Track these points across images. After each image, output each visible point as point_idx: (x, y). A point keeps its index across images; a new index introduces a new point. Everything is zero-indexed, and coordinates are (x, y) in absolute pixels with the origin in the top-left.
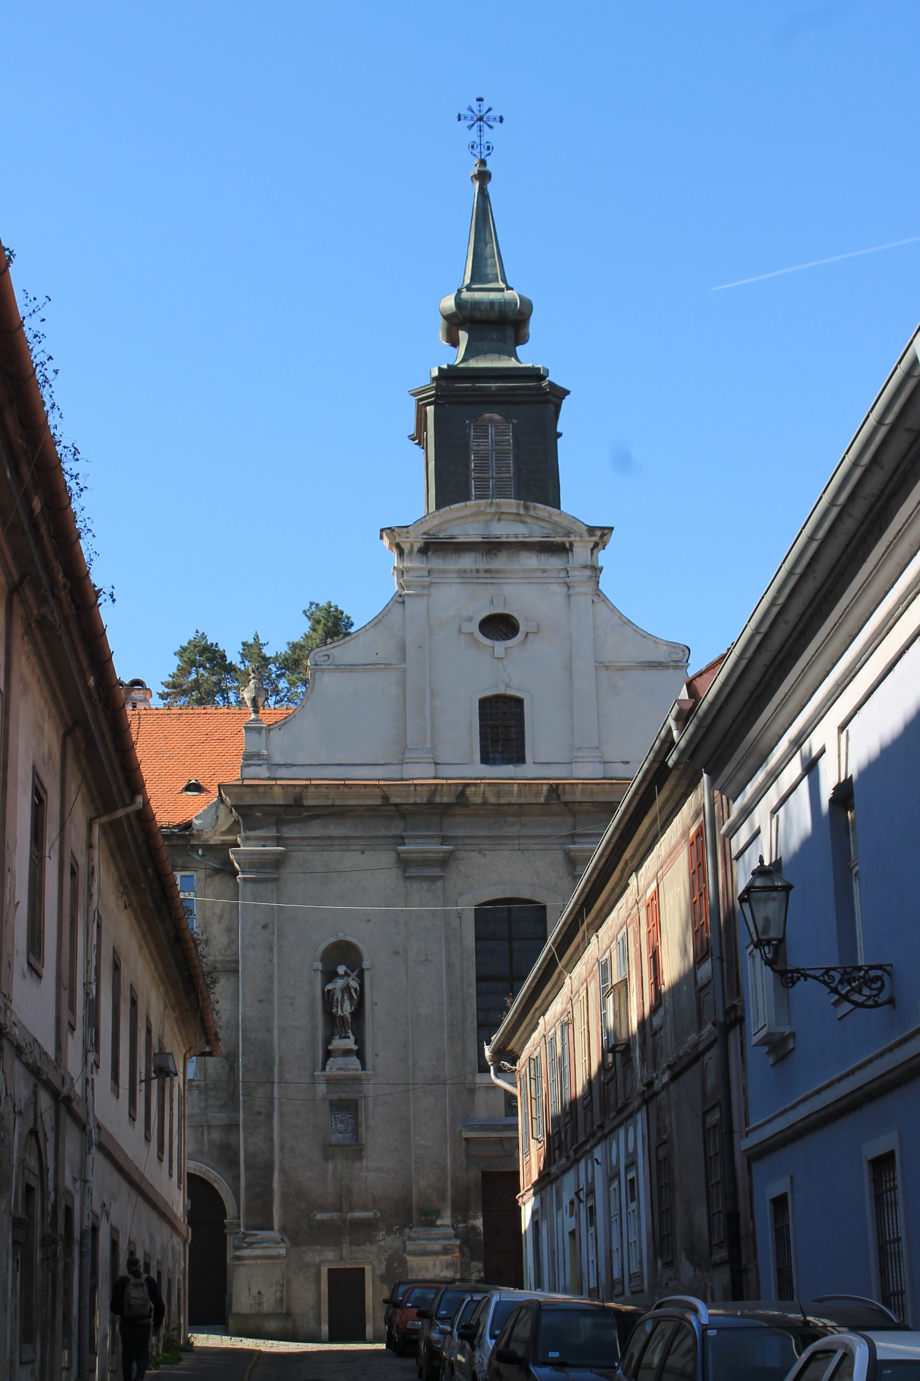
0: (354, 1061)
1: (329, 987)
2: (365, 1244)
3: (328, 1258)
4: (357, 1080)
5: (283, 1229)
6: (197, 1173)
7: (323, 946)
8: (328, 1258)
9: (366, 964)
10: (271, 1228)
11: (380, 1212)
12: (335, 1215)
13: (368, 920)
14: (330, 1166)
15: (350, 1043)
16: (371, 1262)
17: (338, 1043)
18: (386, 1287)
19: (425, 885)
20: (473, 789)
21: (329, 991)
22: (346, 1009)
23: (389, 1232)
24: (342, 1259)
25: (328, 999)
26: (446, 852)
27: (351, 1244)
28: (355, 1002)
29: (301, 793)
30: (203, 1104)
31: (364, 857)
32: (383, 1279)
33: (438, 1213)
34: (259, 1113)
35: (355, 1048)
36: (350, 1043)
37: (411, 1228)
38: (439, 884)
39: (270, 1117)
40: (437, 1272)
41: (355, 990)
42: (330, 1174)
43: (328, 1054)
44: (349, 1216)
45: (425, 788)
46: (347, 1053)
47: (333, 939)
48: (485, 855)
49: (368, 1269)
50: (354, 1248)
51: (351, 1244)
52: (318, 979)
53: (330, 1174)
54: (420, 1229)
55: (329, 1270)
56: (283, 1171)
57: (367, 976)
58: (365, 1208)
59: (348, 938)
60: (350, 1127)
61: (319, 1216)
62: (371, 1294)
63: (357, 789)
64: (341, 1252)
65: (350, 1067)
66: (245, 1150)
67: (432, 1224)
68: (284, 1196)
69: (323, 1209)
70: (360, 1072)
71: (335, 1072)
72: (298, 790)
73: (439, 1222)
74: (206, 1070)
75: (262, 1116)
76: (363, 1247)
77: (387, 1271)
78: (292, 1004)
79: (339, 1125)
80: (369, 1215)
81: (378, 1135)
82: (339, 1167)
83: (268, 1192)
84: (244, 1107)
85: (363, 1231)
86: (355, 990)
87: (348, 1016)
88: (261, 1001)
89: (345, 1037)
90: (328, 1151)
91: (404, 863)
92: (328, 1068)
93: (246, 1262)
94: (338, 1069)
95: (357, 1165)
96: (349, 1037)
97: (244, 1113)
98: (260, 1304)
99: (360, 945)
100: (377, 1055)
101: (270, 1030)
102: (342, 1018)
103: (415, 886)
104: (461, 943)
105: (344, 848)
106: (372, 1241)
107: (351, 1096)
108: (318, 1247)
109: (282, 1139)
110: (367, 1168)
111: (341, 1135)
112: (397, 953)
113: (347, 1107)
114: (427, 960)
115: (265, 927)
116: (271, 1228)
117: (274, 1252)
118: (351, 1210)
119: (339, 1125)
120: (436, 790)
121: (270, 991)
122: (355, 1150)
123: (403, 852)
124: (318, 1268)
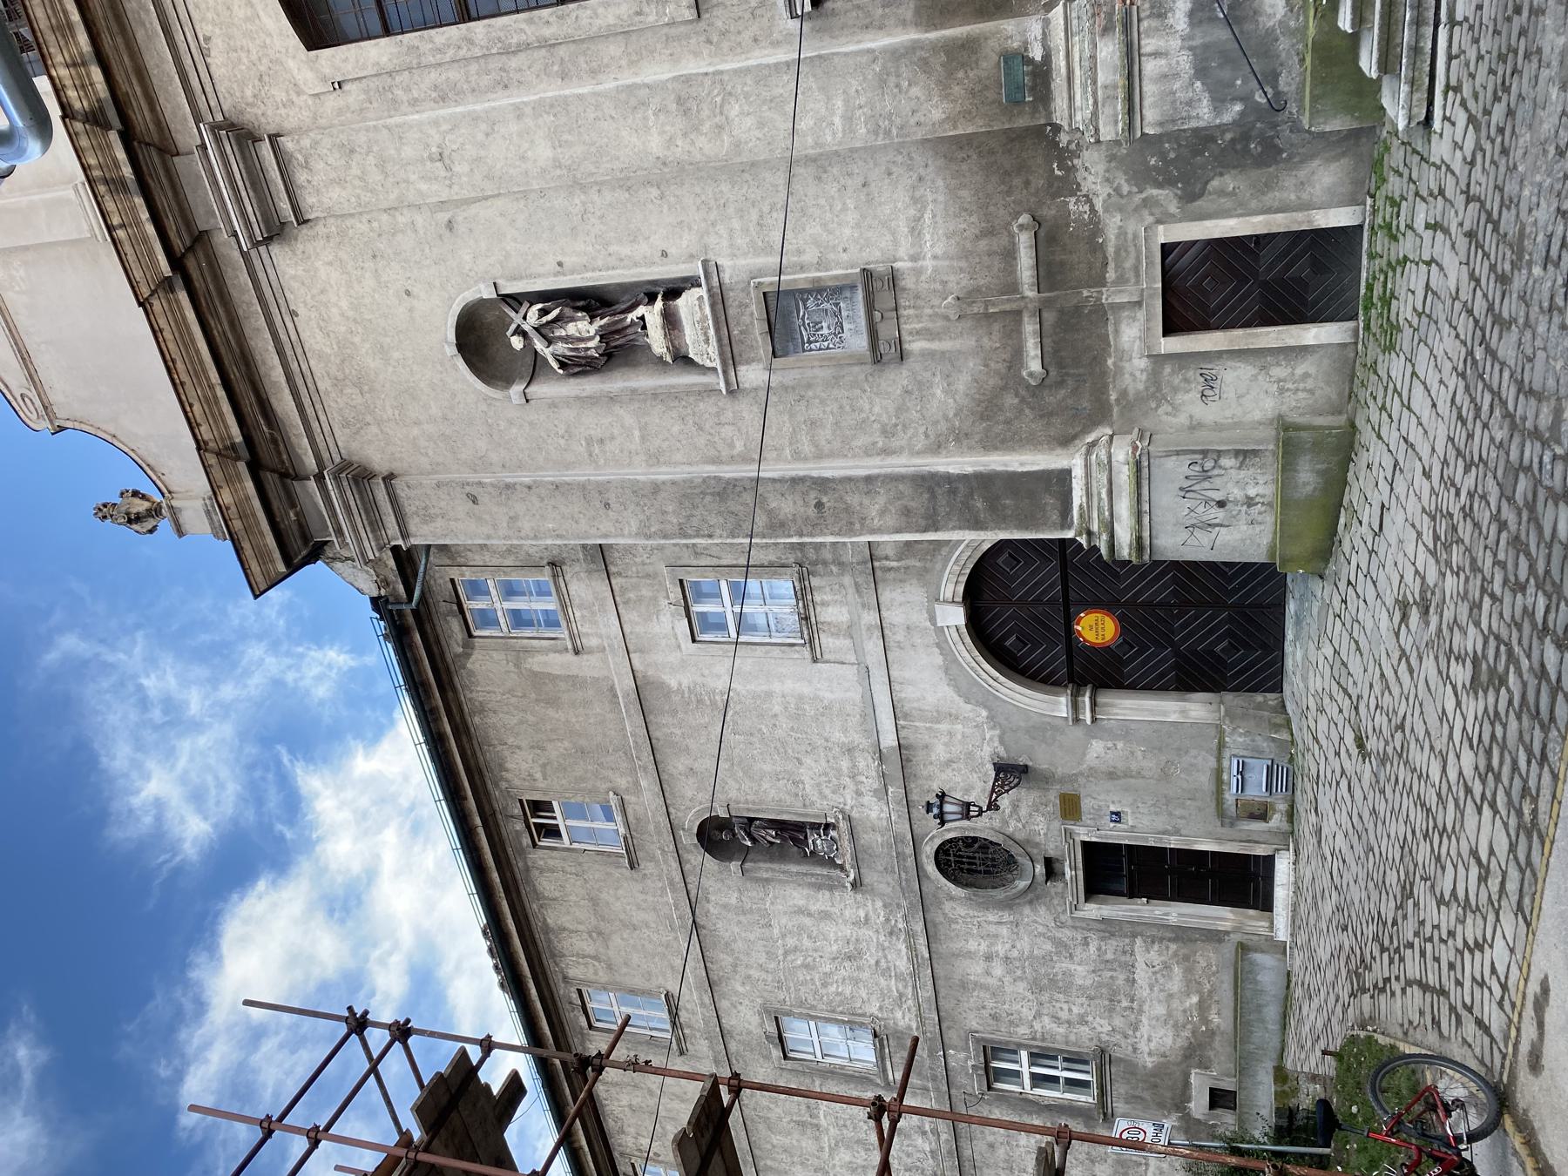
0: (687, 304)
1: (555, 365)
2: (1101, 248)
3: (1136, 336)
4: (719, 300)
5: (1066, 441)
6: (964, 579)
7: (479, 385)
8: (1136, 336)
9: (488, 293)
10: (1065, 476)
11: (1017, 215)
12: (1030, 327)
13: (408, 293)
14: (915, 346)
15: (652, 314)
16: (1144, 229)
17: (656, 339)
18: (1215, 183)
19: (301, 177)
20: (72, 93)
21: (563, 365)
22: (584, 329)
23: (1068, 185)
24: (1139, 304)
25: (576, 366)
26: (218, 140)
27: (1101, 282)
28: (568, 311)
29: (218, 454)
30: (835, 569)
31: (301, 311)
32: (1190, 197)
33: (1014, 58)
34: (819, 505)
35: (659, 304)
36: (652, 314)
37: (1057, 129)
38: (287, 143)
39: (822, 484)
40: (1175, 43)
41: (543, 312)
42: (935, 345)
43: (682, 360)
44: (1030, 293)
45: (110, 205)
46: (671, 321)
47: (460, 363)
48: (208, 39)
49: (1164, 235)
50: (1111, 275)
51: (1101, 282)
52: (543, 390)
53: (935, 345)
54: (1060, 104)
55: (1168, 331)
56: (937, 448)
57: (509, 288)
58: (1010, 254)
59: (452, 336)
60: (826, 305)
61: (1035, 366)
62: (1232, 222)
63: (172, 346)
64: (1121, 306)
65: (698, 316)
66: (898, 531)
67: (1042, 73)
68: (990, 443)
69: (1018, 355)
70: (702, 291)
71: (713, 349)
72: (212, 460)
73: (1037, 53)
74: (771, 565)
75: (825, 500)
76: (1111, 250)
77: (1169, 182)
78: (602, 441)
79: (825, 331)
80: (1024, 241)
81: (838, 235)
82: (918, 326)
83: (984, 482)
84: (812, 535)
85: (1067, 257)
86: (543, 312)
87: (599, 322)
88: (607, 505)
89: (644, 327)
90: (884, 351)
91: (274, 232)
92: (708, 364)
93: (1146, 534)
94: (707, 341)
95: (907, 282)
96: (642, 318)
97: (822, 534)
98: (1250, 502)
99: (456, 309)
100: (664, 254)
101: (656, 488)
102: (605, 336)
103: (309, 200)
104: (390, 74)
105: (299, 351)
106: (1094, 227)
107: (755, 310)
108: (1110, 362)
109: (868, 452)
110: (914, 258)
111: (846, 326)
112: (450, 225)
113: (784, 315)
114: (441, 159)
115: (475, 501)
116: (1065, 476)
117: (1124, 476)
118: (1012, 288)
119: (825, 331)
120: (106, 182)
121: (583, 487)
122: (878, 287)
123: (251, 236)
124: (1158, 360)
